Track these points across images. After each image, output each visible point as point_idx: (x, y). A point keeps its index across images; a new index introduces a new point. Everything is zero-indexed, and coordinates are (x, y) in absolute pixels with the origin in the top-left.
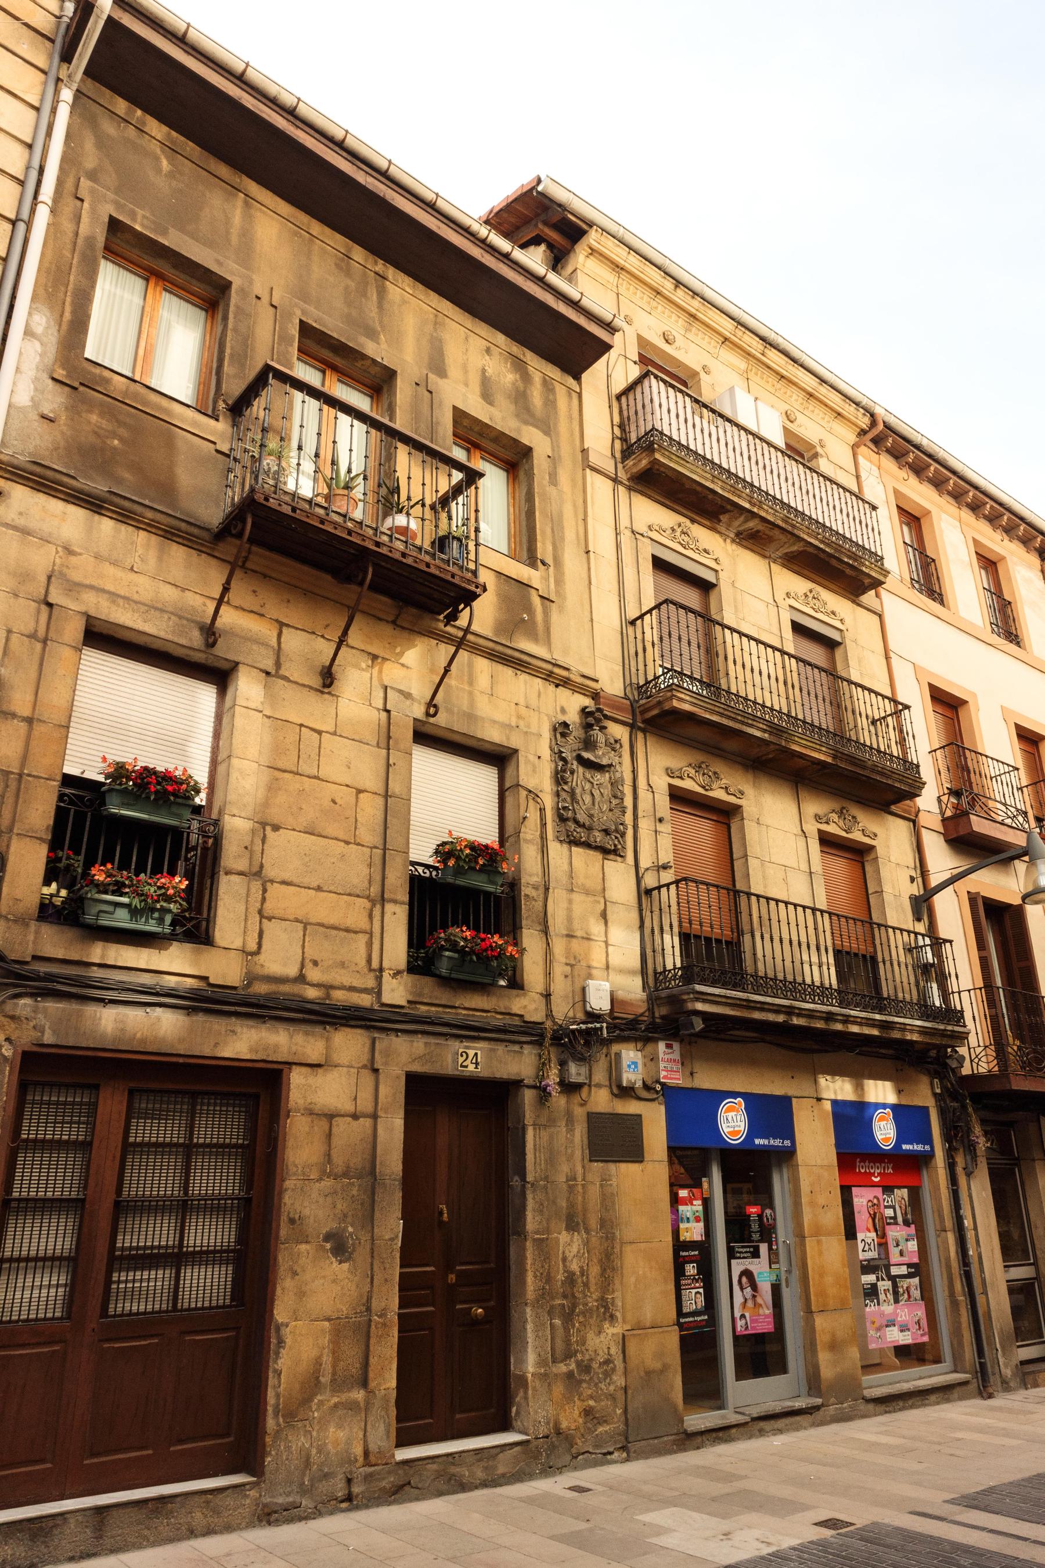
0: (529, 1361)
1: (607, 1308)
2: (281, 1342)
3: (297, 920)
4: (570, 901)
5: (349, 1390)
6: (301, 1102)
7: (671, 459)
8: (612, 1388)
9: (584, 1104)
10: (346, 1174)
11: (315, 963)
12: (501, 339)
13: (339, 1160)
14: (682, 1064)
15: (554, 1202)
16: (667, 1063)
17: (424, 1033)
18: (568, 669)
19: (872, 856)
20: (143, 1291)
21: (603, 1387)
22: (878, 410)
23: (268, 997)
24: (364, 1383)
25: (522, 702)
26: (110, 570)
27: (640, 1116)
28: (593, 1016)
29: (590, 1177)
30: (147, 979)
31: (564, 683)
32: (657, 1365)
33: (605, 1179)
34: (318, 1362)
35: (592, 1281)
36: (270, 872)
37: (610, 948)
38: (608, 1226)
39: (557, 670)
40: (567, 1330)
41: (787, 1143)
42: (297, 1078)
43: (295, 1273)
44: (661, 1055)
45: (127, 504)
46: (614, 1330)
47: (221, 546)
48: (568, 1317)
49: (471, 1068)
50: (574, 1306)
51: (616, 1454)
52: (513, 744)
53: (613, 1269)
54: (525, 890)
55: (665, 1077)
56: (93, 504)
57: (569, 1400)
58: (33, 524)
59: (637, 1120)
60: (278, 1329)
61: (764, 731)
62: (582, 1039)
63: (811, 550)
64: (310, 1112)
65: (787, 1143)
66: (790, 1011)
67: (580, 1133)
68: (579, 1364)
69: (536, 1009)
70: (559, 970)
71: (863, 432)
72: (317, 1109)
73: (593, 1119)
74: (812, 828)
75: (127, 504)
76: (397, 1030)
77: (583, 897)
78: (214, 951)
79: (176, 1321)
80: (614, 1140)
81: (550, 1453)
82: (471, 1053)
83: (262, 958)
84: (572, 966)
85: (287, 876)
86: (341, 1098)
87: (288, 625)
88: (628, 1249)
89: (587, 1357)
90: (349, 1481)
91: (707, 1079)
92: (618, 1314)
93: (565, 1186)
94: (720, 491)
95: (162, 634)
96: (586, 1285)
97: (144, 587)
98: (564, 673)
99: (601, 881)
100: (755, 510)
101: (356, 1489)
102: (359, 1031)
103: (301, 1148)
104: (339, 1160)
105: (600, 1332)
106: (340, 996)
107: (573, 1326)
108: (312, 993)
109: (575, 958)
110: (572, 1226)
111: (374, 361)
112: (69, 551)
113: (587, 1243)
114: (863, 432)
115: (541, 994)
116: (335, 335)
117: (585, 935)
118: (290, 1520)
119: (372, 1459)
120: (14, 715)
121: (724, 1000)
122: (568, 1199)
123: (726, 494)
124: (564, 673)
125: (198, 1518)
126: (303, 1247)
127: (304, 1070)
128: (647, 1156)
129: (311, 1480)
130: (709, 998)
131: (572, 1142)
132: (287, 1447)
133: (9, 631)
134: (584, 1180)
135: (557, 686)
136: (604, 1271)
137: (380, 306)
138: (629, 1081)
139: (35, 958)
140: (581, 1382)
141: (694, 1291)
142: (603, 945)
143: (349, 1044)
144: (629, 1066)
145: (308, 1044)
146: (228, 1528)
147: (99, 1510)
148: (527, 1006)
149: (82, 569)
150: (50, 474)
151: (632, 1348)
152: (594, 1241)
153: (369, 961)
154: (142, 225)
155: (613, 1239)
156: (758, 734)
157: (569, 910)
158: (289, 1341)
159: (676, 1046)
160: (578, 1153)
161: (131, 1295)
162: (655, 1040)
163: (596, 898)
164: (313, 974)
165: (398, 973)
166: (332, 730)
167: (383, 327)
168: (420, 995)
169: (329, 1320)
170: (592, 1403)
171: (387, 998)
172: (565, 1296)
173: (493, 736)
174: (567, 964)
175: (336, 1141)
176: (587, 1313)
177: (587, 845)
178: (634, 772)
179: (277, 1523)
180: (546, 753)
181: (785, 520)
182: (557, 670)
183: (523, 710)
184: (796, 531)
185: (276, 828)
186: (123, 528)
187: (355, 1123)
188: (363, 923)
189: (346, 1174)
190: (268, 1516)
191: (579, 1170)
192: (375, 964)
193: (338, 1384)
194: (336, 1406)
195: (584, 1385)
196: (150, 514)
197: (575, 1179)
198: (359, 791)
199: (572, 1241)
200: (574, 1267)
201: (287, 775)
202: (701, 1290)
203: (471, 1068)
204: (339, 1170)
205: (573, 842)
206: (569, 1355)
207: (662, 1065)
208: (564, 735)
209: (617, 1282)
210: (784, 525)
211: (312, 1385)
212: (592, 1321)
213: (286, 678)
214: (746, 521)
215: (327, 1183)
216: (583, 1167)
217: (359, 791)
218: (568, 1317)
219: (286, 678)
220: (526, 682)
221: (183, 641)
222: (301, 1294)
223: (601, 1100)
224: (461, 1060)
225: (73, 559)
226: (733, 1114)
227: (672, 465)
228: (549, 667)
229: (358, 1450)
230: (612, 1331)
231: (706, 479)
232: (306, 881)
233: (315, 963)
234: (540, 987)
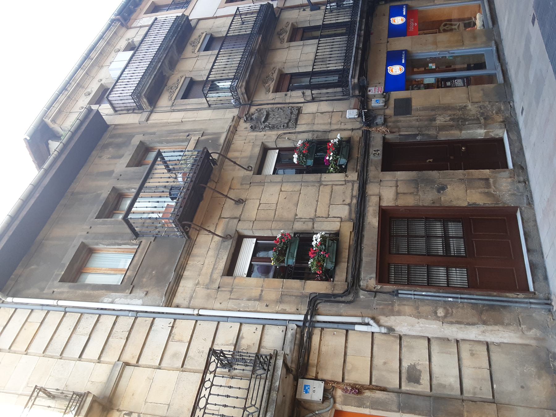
0: (480, 133)
1: (462, 108)
2: (474, 204)
3: (329, 207)
4: (318, 124)
5: (490, 183)
6: (393, 202)
9: (390, 117)
10: (417, 188)
11: (344, 201)
12: (94, 153)
13: (412, 190)
16: (375, 90)
17: (367, 167)
19: (295, 24)
20: (458, 246)
22: (113, 17)
24: (487, 179)
26: (204, 271)
27: (395, 100)
28: (360, 115)
32: (481, 92)
33: (417, 110)
34: (481, 193)
35: (453, 113)
36: (312, 216)
38: (433, 109)
39: (231, 130)
40: (470, 120)
41: (404, 52)
42: (384, 204)
45: (178, 267)
46: (470, 107)
47: (192, 237)
48: (465, 120)
50: (462, 118)
51: (511, 104)
56: (179, 278)
58: (188, 296)
59: (395, 100)
60: (470, 205)
61: (251, 58)
63: (175, 42)
65: (404, 52)
66: (357, 48)
67: (401, 118)
68: (481, 116)
71: (122, 25)
73: (396, 113)
74: (286, 45)
75: (178, 267)
76: (367, 175)
78: (341, 230)
79: (467, 237)
80: (404, 107)
81: (511, 125)
82: (374, 152)
83: (343, 217)
84: (341, 123)
85: (313, 211)
87: (220, 216)
88: (442, 102)
90: (519, 182)
92: (464, 104)
95: (227, 253)
96: (454, 115)
97: (209, 260)
98: (232, 127)
101: (521, 179)
102: (367, 187)
103: (409, 201)
106: (355, 193)
108: (355, 201)
110: (435, 120)
111: (110, 194)
113: (440, 115)
114: (122, 25)
116: (100, 207)
118: (532, 198)
120: (261, 295)
124: (232, 127)
125: (531, 224)
126: (442, 199)
127: (381, 201)
129: (519, 193)
132: (508, 200)
133: (230, 299)
136: (450, 110)
140: (487, 115)
143: (372, 189)
146: (534, 215)
147: (528, 251)
149: (205, 279)
150: (169, 291)
153: (342, 185)
154: (62, 271)
156: (253, 60)
157: (321, 124)
159: (369, 89)
160: (408, 119)
161: (459, 250)
162: (368, 95)
164: (348, 201)
165: (346, 176)
168: (354, 169)
169: (466, 191)
170: (494, 112)
172: (458, 121)
175: (405, 192)
176: (463, 114)
177: (297, 120)
178: (268, 104)
179: (533, 201)
180: (263, 133)
181: (165, 50)
182: (231, 130)
184: (169, 46)
185: (296, 215)
186: (187, 268)
190: (530, 203)
191: (414, 118)
192: (344, 183)
193: (488, 186)
194: (495, 187)
196: (182, 259)
198: (281, 191)
200: (448, 118)
201: (277, 213)
203: (379, 152)
204: (416, 190)
206: (478, 119)
207: (376, 93)
208: (255, 128)
210: (167, 51)
211: (488, 194)
213: (241, 215)
215: (420, 193)
217: (281, 191)
218: (465, 120)
219: (241, 215)
221: (229, 247)
223: (390, 111)
225: (200, 282)
228: (230, 132)
229: (510, 180)
230: (470, 106)
232: (315, 205)
233: (344, 201)
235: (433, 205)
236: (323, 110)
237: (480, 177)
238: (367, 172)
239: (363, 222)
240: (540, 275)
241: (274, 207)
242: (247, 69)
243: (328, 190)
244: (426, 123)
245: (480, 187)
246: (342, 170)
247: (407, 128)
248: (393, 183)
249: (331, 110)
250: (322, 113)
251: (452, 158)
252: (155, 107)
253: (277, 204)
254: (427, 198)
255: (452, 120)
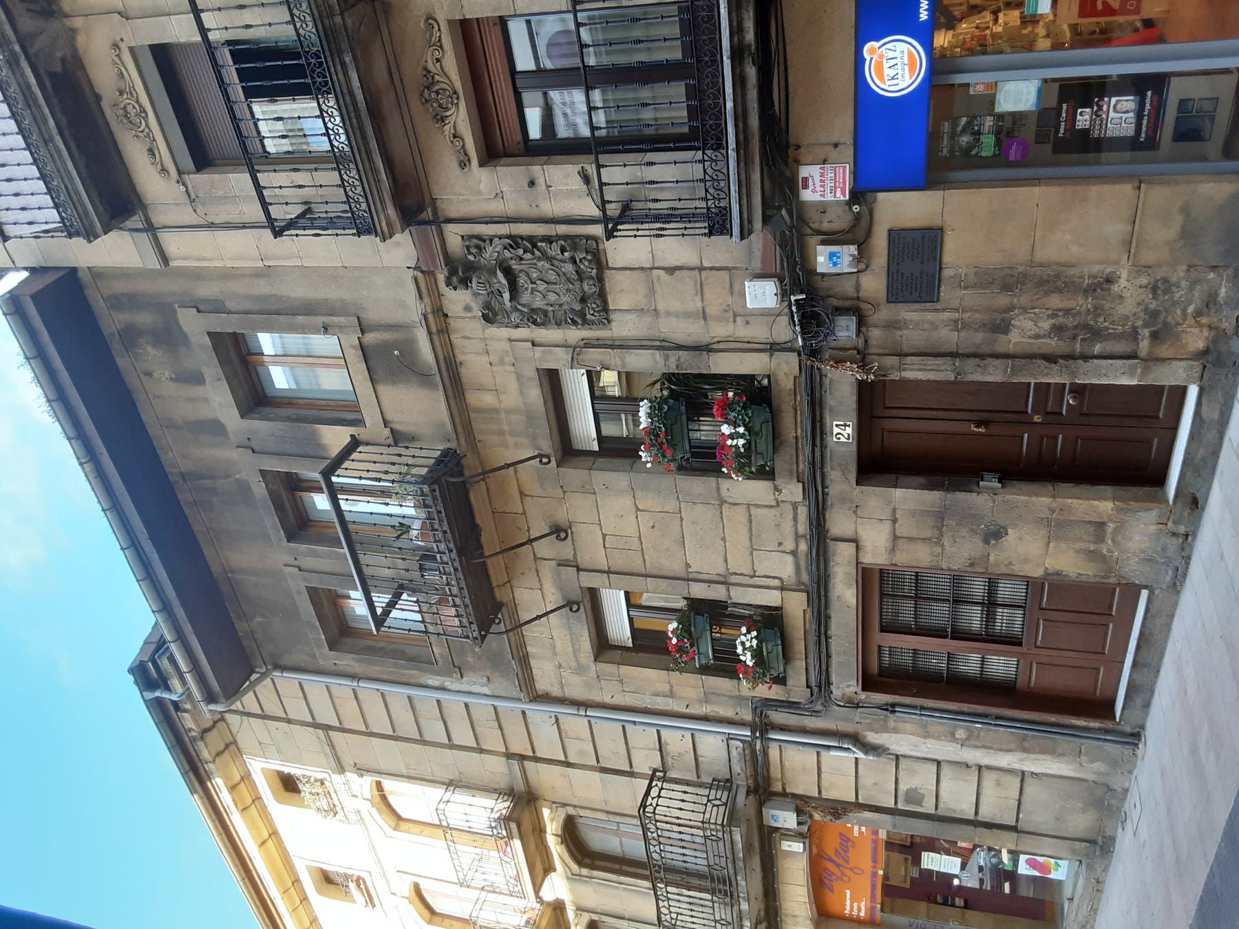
1: (1100, 284)
2: (1058, 573)
3: (751, 554)
4: (668, 314)
5: (1105, 532)
7: (86, 212)
8: (1183, 284)
9: (876, 306)
10: (940, 529)
11: (780, 544)
12: (122, 362)
13: (928, 533)
14: (824, 162)
15: (978, 346)
16: (823, 185)
17: (822, 468)
18: (425, 316)
21: (1178, 295)
23: (810, 573)
25: (485, 358)
26: (559, 648)
28: (784, 294)
29: (955, 304)
30: (812, 639)
31: (440, 313)
32: (1178, 220)
33: (961, 284)
34: (1077, 551)
37: (706, 264)
38: (1008, 281)
39: (434, 329)
42: (868, 559)
43: (1010, 563)
44: (816, 197)
46: (1123, 282)
47: (505, 600)
48: (1096, 334)
49: (849, 430)
52: (534, 375)
53: (1057, 276)
54: (673, 369)
55: (843, 194)
57: (1178, 337)
61: (343, 64)
62: (812, 306)
64: (893, 550)
66: (738, 54)
67: (909, 313)
68: (1145, 326)
69: (787, 363)
70: (742, 332)
72: (890, 546)
76: (824, 487)
77: (659, 297)
78: (785, 606)
80: (917, 264)
85: (721, 560)
86: (883, 526)
88: (1041, 255)
89: (1142, 314)
90: (1174, 534)
91: (842, 126)
92: (1108, 270)
93: (963, 334)
94: (52, 123)
96: (1067, 312)
98: (430, 317)
99: (635, 273)
100: (17, 48)
101: (1182, 529)
102: (827, 516)
103: (918, 556)
104: (928, 533)
105: (1121, 297)
106: (803, 528)
107: (1107, 328)
108: (803, 547)
109: (726, 311)
110: (1003, 327)
112: (560, 666)
113: (1025, 310)
115: (771, 356)
116: (276, 518)
117: (699, 297)
118: (1185, 575)
119: (1164, 521)
121: (744, 190)
122: (976, 330)
123: (46, 111)
124: (430, 317)
126: (991, 558)
127: (861, 554)
128: (937, 222)
130: (745, 216)
131: (917, 324)
134: (958, 310)
135: (446, 316)
137: (212, 477)
138: (850, 265)
139: (808, 686)
140: (1165, 324)
141: (1112, 114)
142: (704, 273)
143: (839, 523)
144: (835, 264)
145: (842, 555)
147: (1135, 664)
148: (786, 369)
151: (1148, 257)
152: (1024, 300)
153: (771, 507)
155: (1025, 275)
156: (354, 76)
157: (677, 315)
158: (1058, 568)
159: (804, 171)
160: (929, 316)
161: (1011, 623)
162: (801, 205)
163: (655, 280)
165: (776, 489)
166: (598, 528)
167: (228, 477)
168: (791, 473)
169: (1049, 543)
170: (1191, 309)
171: (798, 496)
172: (1074, 338)
173: (535, 395)
174: (735, 321)
175: (914, 534)
176: (1097, 311)
177: (602, 295)
180: (523, 332)
182: (434, 329)
183: (494, 358)
187: (900, 521)
188: (742, 510)
189: (940, 529)
191: (945, 316)
193: (1100, 538)
194: (1113, 541)
195: (1169, 319)
197: (956, 321)
199: (1018, 327)
200: (1046, 325)
202: (1114, 100)
204: (936, 532)
205: (606, 310)
206: (1134, 335)
207: (829, 197)
209: (1071, 272)
211: (1094, 556)
212: (1107, 307)
213: (575, 555)
214: (34, 36)
215: (946, 541)
216: (944, 310)
217: (638, 509)
218: (1096, 334)
219: (575, 555)
220: (463, 353)
222: (1026, 560)
223: (874, 284)
224: (843, 439)
226: (886, 65)
227: (90, 207)
228: (435, 338)
230: (1123, 283)
231: (57, 149)
233: (780, 544)
234: (764, 357)
235: (969, 569)
236: (672, 262)
237: (1087, 519)
238: (824, 487)
239: (826, 591)
240: (1139, 701)
241: (636, 546)
242: (369, 153)
243: (740, 515)
244: (979, 337)
245: (1080, 539)
246: (766, 474)
247: (925, 342)
248: (887, 515)
249: (693, 260)
250: (671, 270)
251: (1037, 419)
252: (143, 207)
253: (640, 538)
254: (960, 551)
255: (1058, 330)
